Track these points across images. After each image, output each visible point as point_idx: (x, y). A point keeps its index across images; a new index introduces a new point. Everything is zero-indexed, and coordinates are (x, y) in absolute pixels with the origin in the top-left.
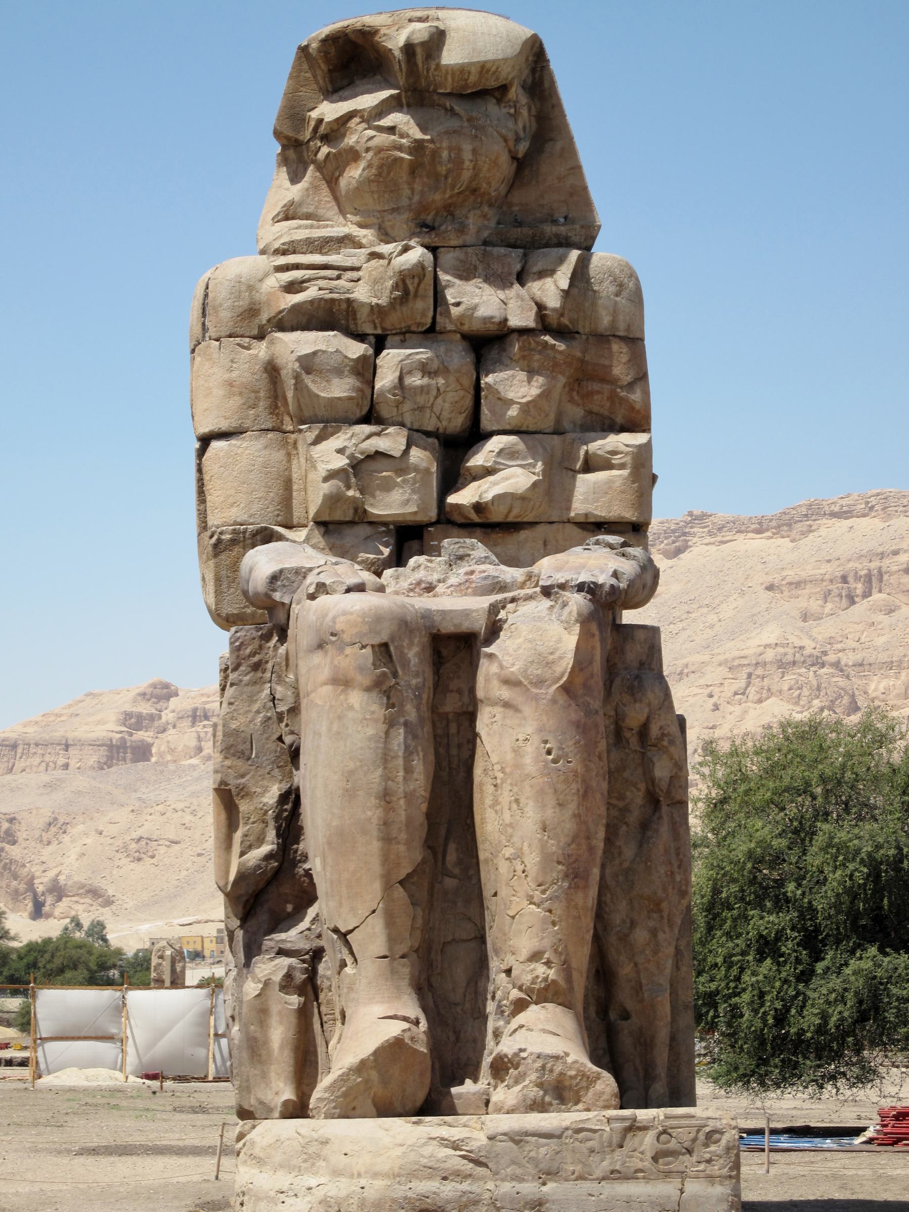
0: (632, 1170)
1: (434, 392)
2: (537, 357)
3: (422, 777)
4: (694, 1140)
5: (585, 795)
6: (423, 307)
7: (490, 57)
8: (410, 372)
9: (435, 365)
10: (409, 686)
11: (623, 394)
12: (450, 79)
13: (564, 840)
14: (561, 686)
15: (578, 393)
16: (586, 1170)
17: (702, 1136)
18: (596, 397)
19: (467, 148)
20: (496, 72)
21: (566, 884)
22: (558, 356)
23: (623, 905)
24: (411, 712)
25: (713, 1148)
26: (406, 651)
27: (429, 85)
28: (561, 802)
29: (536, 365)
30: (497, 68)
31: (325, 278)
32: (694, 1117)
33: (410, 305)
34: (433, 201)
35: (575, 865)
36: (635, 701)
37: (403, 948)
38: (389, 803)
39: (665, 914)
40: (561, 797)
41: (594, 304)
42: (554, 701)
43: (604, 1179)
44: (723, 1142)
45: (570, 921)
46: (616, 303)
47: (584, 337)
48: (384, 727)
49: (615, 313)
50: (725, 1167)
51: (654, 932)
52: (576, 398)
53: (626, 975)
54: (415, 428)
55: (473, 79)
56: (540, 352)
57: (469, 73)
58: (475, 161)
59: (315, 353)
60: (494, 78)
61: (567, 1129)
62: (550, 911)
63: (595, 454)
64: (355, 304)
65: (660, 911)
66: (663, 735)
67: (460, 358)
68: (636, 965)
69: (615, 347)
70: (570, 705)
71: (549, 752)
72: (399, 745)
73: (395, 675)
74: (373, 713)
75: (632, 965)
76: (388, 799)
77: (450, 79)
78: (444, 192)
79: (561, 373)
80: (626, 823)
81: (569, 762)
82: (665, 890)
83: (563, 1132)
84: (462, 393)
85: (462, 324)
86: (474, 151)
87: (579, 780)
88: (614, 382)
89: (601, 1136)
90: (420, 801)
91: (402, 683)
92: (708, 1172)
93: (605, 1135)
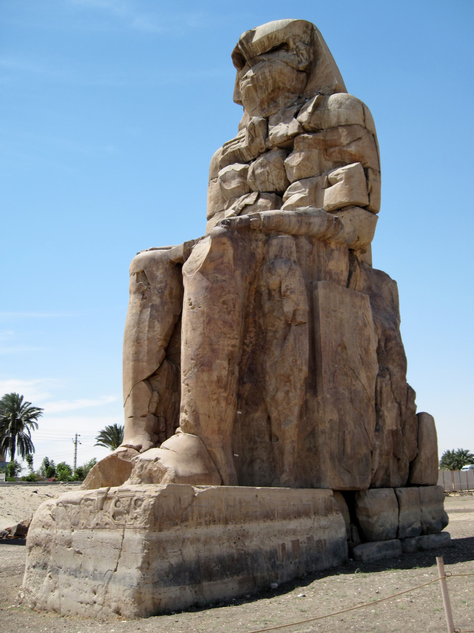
0: (104, 523)
1: (266, 174)
2: (301, 144)
3: (159, 329)
4: (130, 505)
5: (209, 322)
6: (259, 140)
7: (269, 32)
8: (257, 169)
9: (265, 162)
10: (156, 288)
11: (345, 149)
12: (258, 47)
13: (195, 347)
14: (199, 271)
15: (327, 155)
16: (88, 523)
17: (133, 503)
18: (333, 154)
19: (267, 71)
20: (275, 38)
21: (196, 370)
22: (310, 141)
23: (273, 381)
24: (156, 300)
25: (138, 510)
26: (155, 272)
27: (253, 54)
28: (194, 328)
29: (302, 148)
30: (276, 36)
31: (234, 144)
32: (129, 491)
33: (255, 141)
34: (263, 98)
35: (202, 359)
36: (272, 275)
37: (145, 412)
38: (139, 343)
39: (292, 382)
40: (194, 325)
41: (329, 115)
42: (195, 279)
43: (93, 528)
44: (143, 506)
45: (198, 389)
46: (339, 111)
47: (325, 130)
48: (139, 309)
49: (339, 117)
50: (142, 522)
51: (287, 393)
52: (327, 158)
53: (275, 417)
54: (264, 191)
55: (266, 44)
56: (302, 142)
57: (264, 42)
58: (271, 75)
59: (225, 173)
60: (276, 41)
61: (82, 499)
62: (188, 385)
63: (331, 178)
64: (241, 150)
65: (290, 381)
66: (287, 289)
67: (275, 155)
68: (279, 411)
69: (340, 130)
70: (203, 279)
71: (191, 305)
72: (147, 316)
73: (149, 284)
74: (136, 303)
75: (277, 412)
76: (139, 341)
77: (258, 47)
78: (265, 93)
79: (314, 148)
80: (276, 338)
81: (200, 307)
82: (292, 370)
83: (81, 501)
84: (278, 170)
85: (274, 142)
86: (270, 71)
87: (205, 315)
88: (340, 145)
89: (94, 503)
90: (157, 340)
91: (152, 287)
92: (135, 525)
93: (96, 503)
